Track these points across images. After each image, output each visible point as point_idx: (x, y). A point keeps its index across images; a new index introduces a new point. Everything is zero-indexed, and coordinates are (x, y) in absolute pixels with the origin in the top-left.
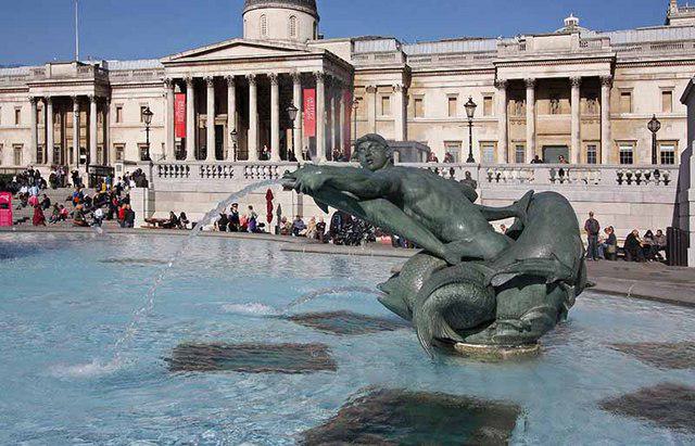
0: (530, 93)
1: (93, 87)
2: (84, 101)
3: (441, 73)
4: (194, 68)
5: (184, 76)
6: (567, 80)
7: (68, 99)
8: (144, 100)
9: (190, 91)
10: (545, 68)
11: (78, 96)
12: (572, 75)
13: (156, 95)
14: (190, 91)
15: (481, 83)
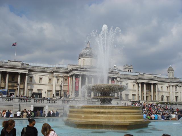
0: (145, 85)
1: (28, 71)
2: (23, 75)
3: (125, 79)
4: (83, 72)
5: (80, 73)
6: (151, 83)
7: (17, 74)
8: (41, 76)
9: (80, 78)
10: (148, 81)
11: (22, 73)
12: (145, 82)
13: (46, 75)
14: (80, 78)
15: (132, 82)
